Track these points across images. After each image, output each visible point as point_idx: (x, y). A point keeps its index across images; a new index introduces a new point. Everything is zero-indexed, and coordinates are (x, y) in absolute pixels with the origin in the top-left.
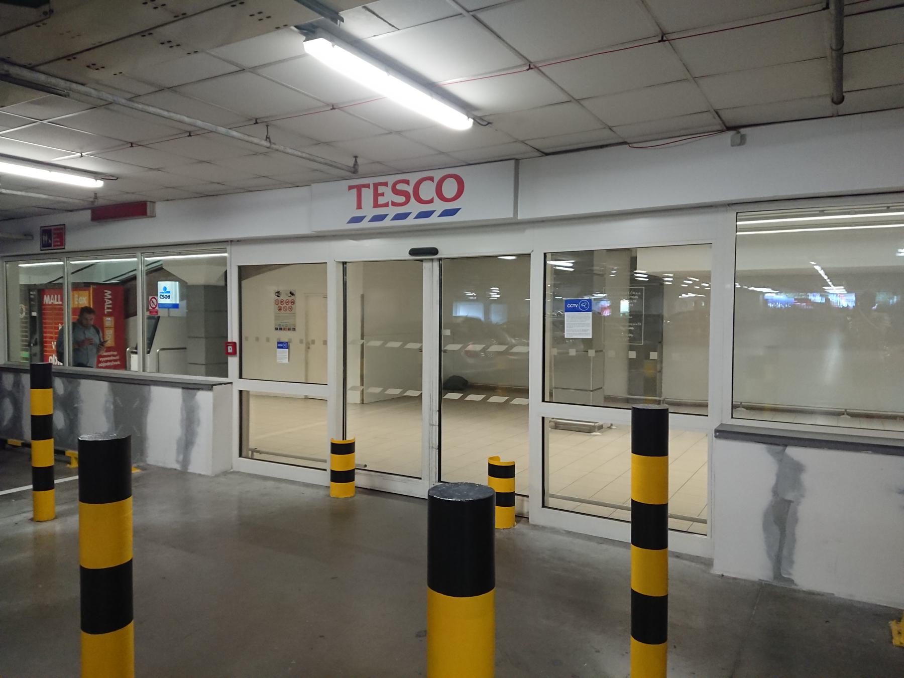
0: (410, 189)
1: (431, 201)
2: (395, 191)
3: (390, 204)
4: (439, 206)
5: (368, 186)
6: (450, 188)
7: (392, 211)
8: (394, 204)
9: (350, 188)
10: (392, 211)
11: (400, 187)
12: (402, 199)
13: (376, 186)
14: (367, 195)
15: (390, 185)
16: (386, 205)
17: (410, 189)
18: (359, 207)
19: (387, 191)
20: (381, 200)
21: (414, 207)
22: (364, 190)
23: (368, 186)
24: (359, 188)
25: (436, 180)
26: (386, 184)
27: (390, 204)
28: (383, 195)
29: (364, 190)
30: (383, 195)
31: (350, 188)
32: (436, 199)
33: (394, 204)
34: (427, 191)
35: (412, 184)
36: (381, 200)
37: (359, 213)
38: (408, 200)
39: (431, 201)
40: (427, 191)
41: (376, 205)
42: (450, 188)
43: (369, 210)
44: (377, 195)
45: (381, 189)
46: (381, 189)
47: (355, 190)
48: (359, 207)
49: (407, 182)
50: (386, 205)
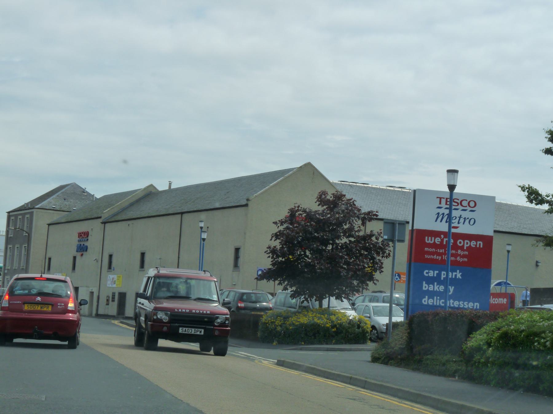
0: (459, 202)
1: (466, 207)
5: (444, 198)
6: (472, 204)
9: (437, 198)
12: (456, 204)
17: (459, 202)
18: (440, 203)
22: (442, 199)
23: (444, 198)
24: (441, 198)
25: (468, 201)
29: (442, 199)
31: (437, 198)
32: (468, 206)
35: (460, 200)
39: (466, 207)
42: (472, 204)
47: (439, 199)
48: (440, 203)
49: (458, 200)
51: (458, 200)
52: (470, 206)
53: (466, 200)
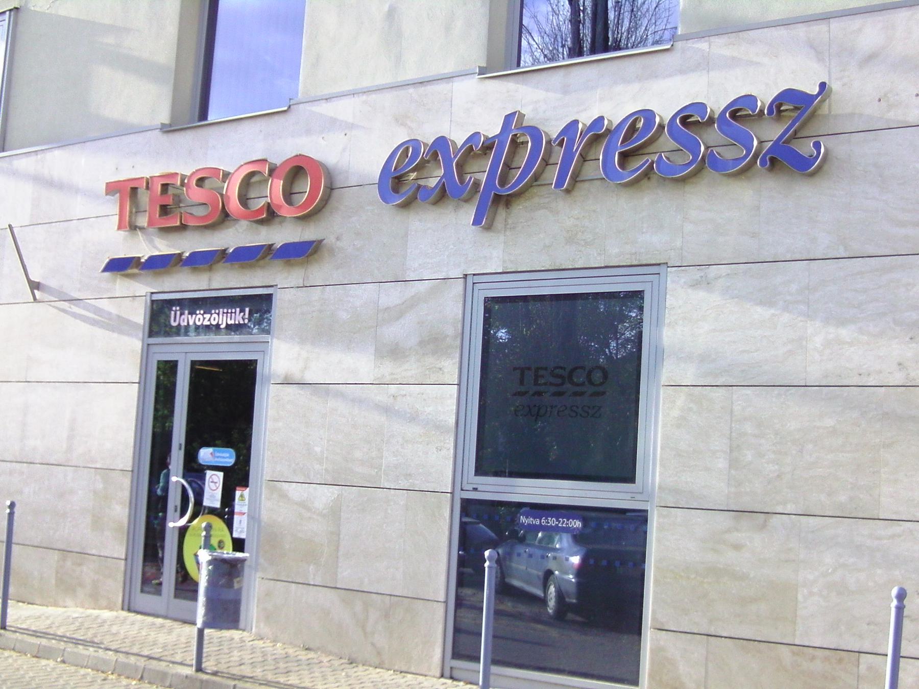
1: (583, 384)
5: (529, 369)
6: (597, 376)
7: (553, 389)
8: (551, 384)
10: (553, 389)
12: (559, 381)
13: (537, 369)
14: (529, 376)
16: (545, 384)
21: (568, 386)
22: (526, 372)
23: (529, 369)
24: (523, 370)
26: (546, 369)
28: (542, 376)
30: (542, 376)
31: (515, 369)
32: (586, 383)
33: (551, 384)
34: (579, 377)
36: (541, 381)
37: (523, 389)
38: (562, 384)
41: (536, 383)
42: (597, 376)
44: (537, 377)
45: (541, 372)
46: (541, 372)
47: (518, 371)
48: (522, 382)
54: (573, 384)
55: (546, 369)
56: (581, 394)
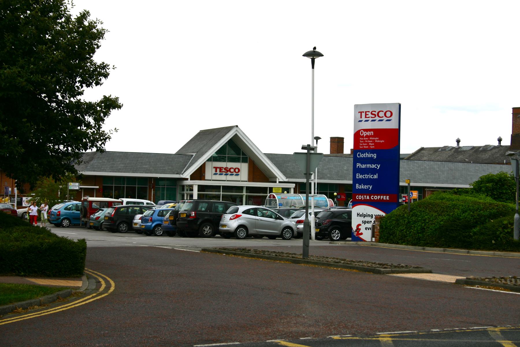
0: (376, 113)
1: (383, 117)
2: (372, 114)
3: (370, 117)
4: (385, 118)
5: (363, 112)
8: (371, 117)
9: (359, 112)
11: (373, 113)
12: (374, 116)
13: (366, 112)
14: (363, 114)
15: (370, 112)
16: (369, 117)
17: (376, 113)
18: (361, 117)
19: (370, 114)
20: (367, 116)
21: (377, 118)
22: (362, 113)
23: (363, 112)
24: (361, 112)
25: (384, 112)
26: (369, 112)
27: (370, 117)
28: (368, 115)
29: (362, 113)
30: (368, 115)
31: (359, 112)
32: (384, 117)
33: (371, 117)
34: (381, 114)
36: (367, 116)
37: (361, 119)
39: (383, 117)
40: (381, 114)
41: (366, 117)
42: (388, 114)
43: (364, 119)
44: (366, 115)
45: (367, 113)
46: (367, 113)
47: (360, 113)
48: (361, 117)
49: (375, 112)
50: (369, 117)
51: (375, 112)
52: (386, 117)
53: (383, 111)
54: (379, 116)
55: (369, 112)
56: (382, 120)
